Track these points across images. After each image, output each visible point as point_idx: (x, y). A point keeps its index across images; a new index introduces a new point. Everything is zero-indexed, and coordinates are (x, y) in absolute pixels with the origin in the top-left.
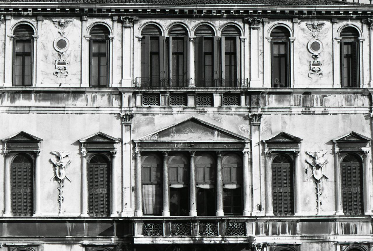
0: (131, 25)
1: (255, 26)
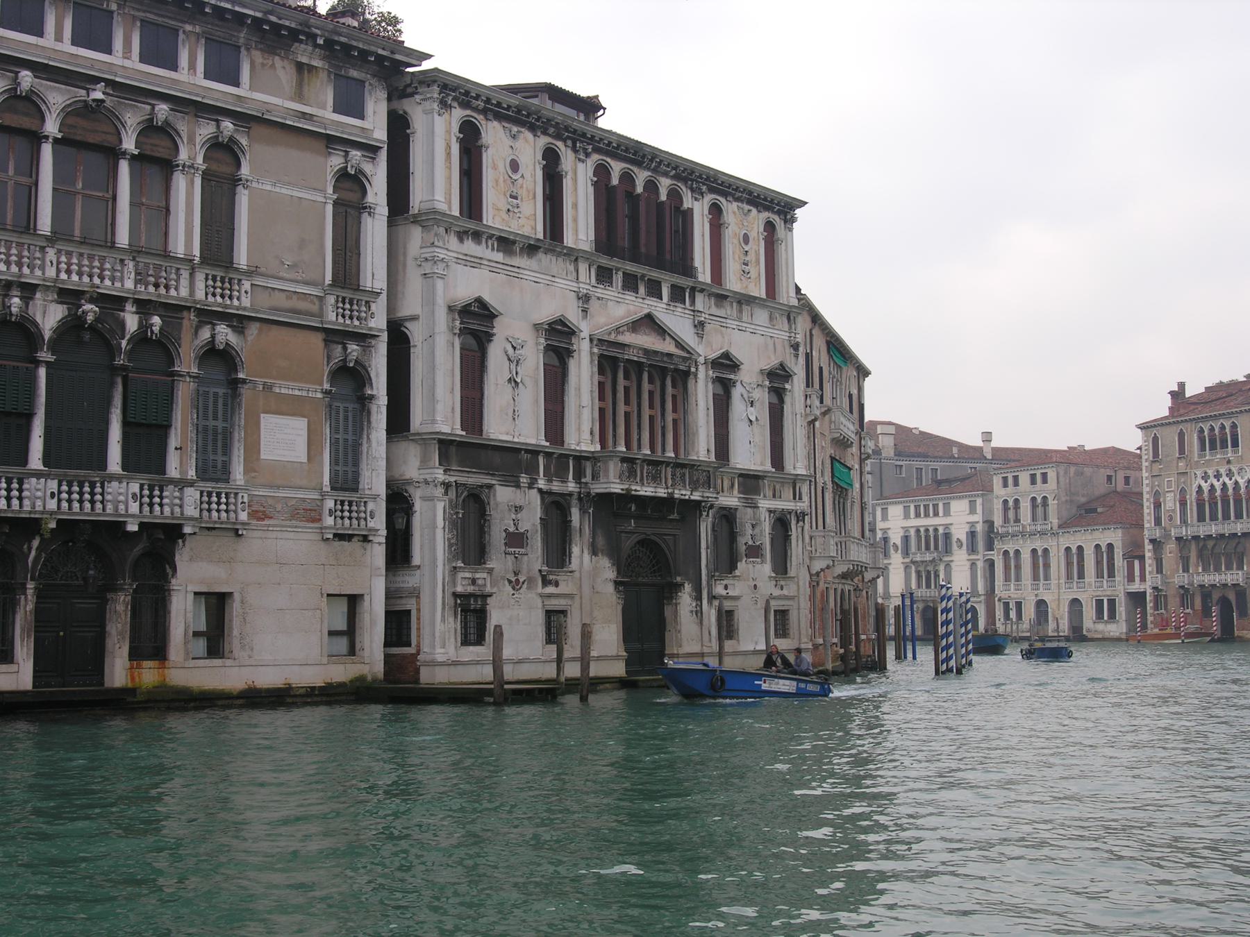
0: (584, 158)
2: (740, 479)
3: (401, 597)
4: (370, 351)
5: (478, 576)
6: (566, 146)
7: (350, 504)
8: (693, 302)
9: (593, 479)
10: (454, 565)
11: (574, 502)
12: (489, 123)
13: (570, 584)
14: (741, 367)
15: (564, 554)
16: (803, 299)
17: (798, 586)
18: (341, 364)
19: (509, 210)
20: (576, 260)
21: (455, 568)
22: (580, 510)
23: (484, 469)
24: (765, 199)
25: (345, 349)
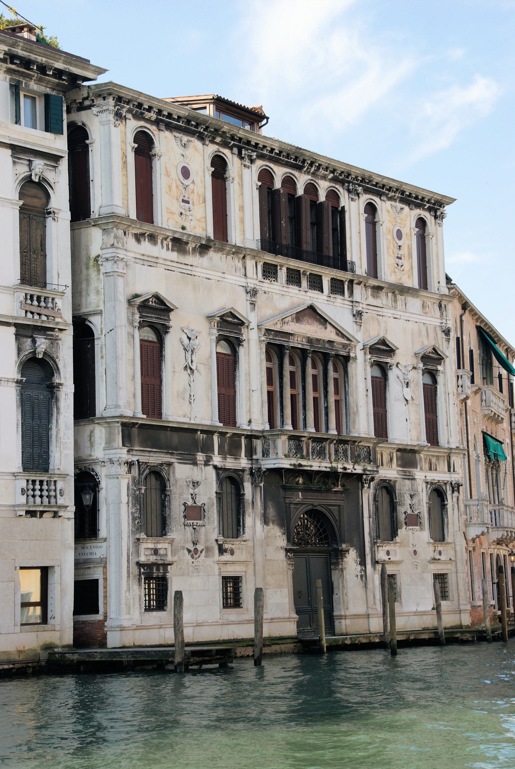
0: (250, 164)
1: (353, 197)
2: (399, 453)
3: (89, 568)
4: (58, 344)
5: (159, 546)
6: (232, 153)
7: (41, 482)
8: (351, 293)
9: (263, 456)
10: (137, 536)
11: (247, 476)
12: (162, 133)
13: (244, 552)
14: (397, 351)
15: (238, 524)
16: (452, 288)
17: (455, 551)
18: (31, 356)
19: (181, 214)
20: (244, 257)
21: (138, 539)
22: (252, 484)
23: (162, 449)
24: (417, 198)
25: (34, 342)
